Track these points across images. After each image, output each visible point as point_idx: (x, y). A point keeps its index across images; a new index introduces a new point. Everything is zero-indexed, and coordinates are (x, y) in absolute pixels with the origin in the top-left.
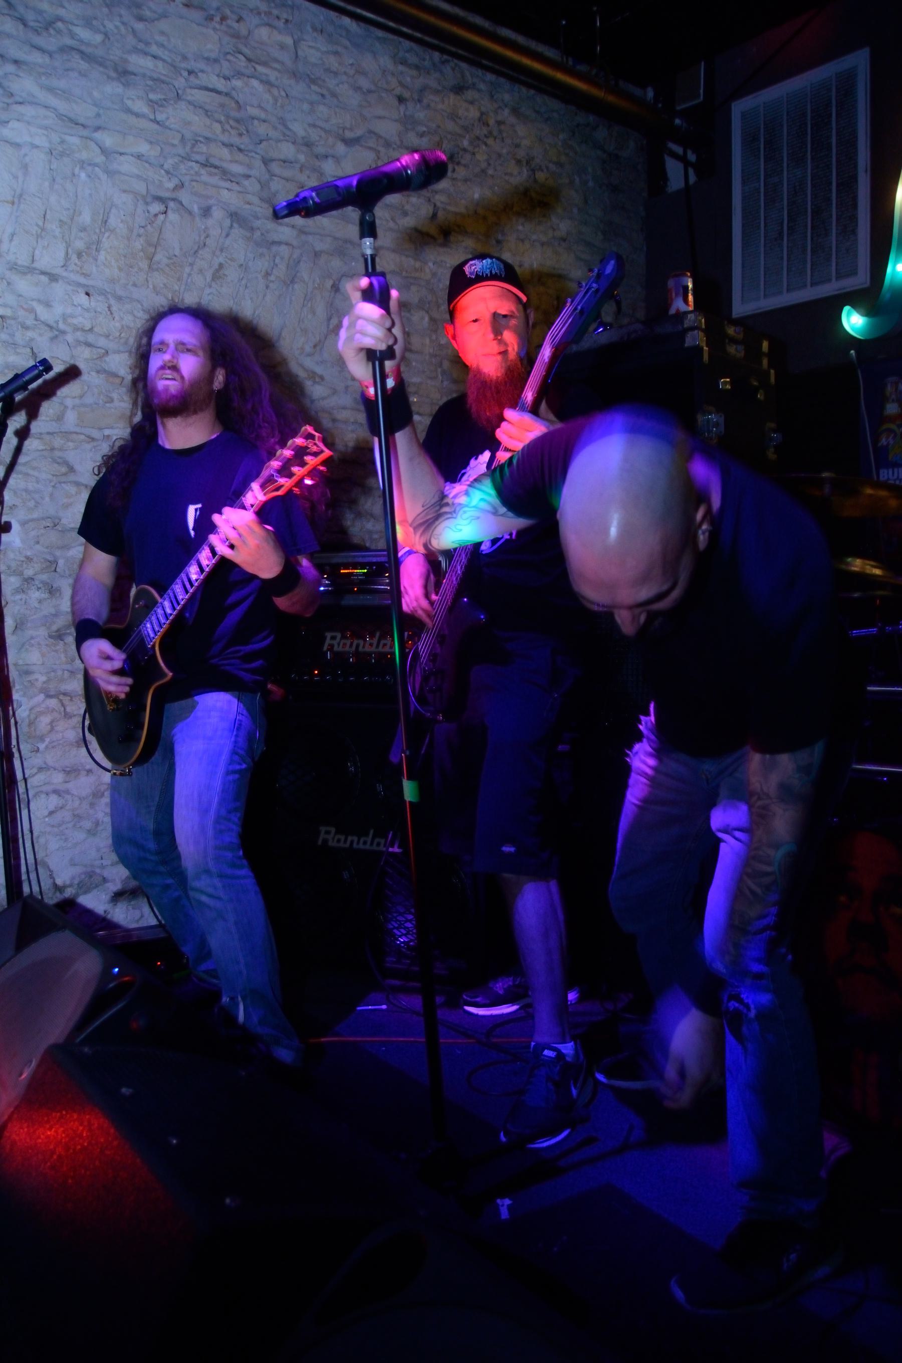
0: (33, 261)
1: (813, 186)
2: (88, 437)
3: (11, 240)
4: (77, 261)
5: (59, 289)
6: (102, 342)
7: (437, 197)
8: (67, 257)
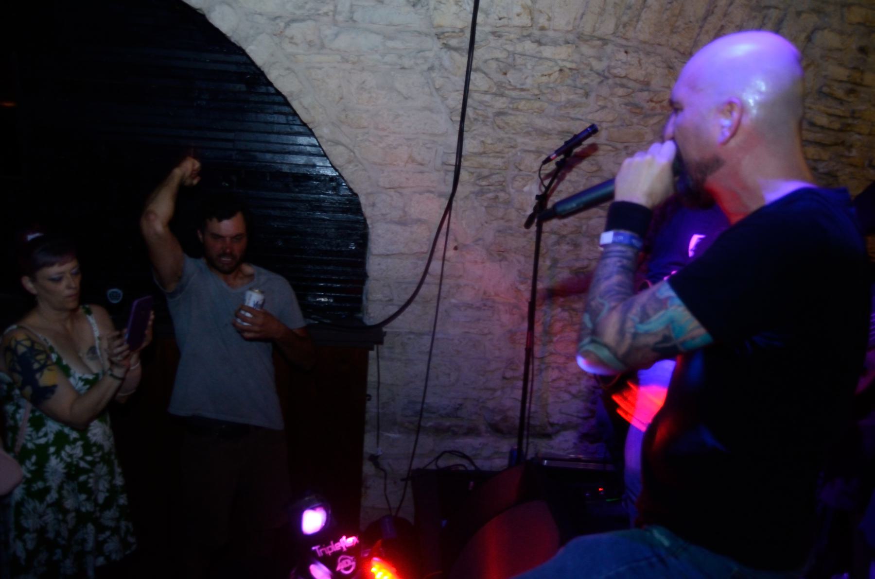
0: (594, 31)
2: (613, 147)
3: (581, 18)
5: (609, 48)
6: (631, 84)
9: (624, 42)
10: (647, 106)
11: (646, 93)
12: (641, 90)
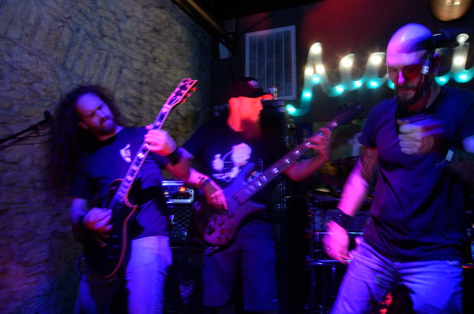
1: (276, 65)
4: (26, 38)
5: (16, 49)
7: (154, 45)
8: (21, 36)
9: (27, 47)
10: (43, 93)
11: (43, 85)
12: (37, 82)
